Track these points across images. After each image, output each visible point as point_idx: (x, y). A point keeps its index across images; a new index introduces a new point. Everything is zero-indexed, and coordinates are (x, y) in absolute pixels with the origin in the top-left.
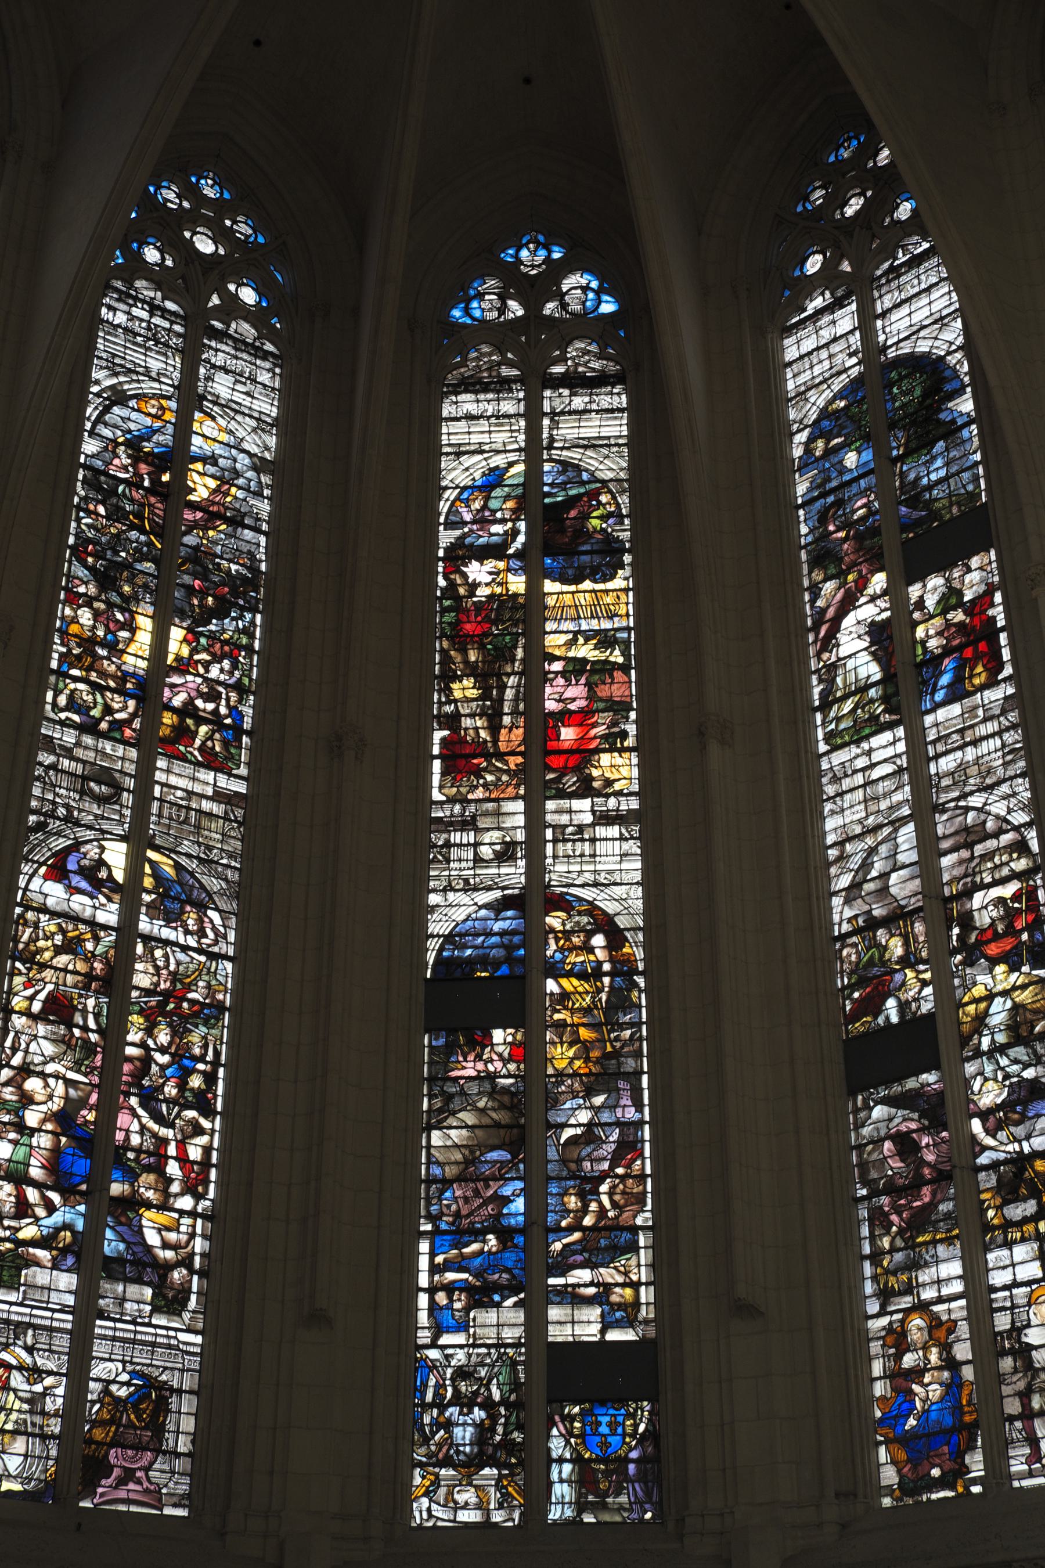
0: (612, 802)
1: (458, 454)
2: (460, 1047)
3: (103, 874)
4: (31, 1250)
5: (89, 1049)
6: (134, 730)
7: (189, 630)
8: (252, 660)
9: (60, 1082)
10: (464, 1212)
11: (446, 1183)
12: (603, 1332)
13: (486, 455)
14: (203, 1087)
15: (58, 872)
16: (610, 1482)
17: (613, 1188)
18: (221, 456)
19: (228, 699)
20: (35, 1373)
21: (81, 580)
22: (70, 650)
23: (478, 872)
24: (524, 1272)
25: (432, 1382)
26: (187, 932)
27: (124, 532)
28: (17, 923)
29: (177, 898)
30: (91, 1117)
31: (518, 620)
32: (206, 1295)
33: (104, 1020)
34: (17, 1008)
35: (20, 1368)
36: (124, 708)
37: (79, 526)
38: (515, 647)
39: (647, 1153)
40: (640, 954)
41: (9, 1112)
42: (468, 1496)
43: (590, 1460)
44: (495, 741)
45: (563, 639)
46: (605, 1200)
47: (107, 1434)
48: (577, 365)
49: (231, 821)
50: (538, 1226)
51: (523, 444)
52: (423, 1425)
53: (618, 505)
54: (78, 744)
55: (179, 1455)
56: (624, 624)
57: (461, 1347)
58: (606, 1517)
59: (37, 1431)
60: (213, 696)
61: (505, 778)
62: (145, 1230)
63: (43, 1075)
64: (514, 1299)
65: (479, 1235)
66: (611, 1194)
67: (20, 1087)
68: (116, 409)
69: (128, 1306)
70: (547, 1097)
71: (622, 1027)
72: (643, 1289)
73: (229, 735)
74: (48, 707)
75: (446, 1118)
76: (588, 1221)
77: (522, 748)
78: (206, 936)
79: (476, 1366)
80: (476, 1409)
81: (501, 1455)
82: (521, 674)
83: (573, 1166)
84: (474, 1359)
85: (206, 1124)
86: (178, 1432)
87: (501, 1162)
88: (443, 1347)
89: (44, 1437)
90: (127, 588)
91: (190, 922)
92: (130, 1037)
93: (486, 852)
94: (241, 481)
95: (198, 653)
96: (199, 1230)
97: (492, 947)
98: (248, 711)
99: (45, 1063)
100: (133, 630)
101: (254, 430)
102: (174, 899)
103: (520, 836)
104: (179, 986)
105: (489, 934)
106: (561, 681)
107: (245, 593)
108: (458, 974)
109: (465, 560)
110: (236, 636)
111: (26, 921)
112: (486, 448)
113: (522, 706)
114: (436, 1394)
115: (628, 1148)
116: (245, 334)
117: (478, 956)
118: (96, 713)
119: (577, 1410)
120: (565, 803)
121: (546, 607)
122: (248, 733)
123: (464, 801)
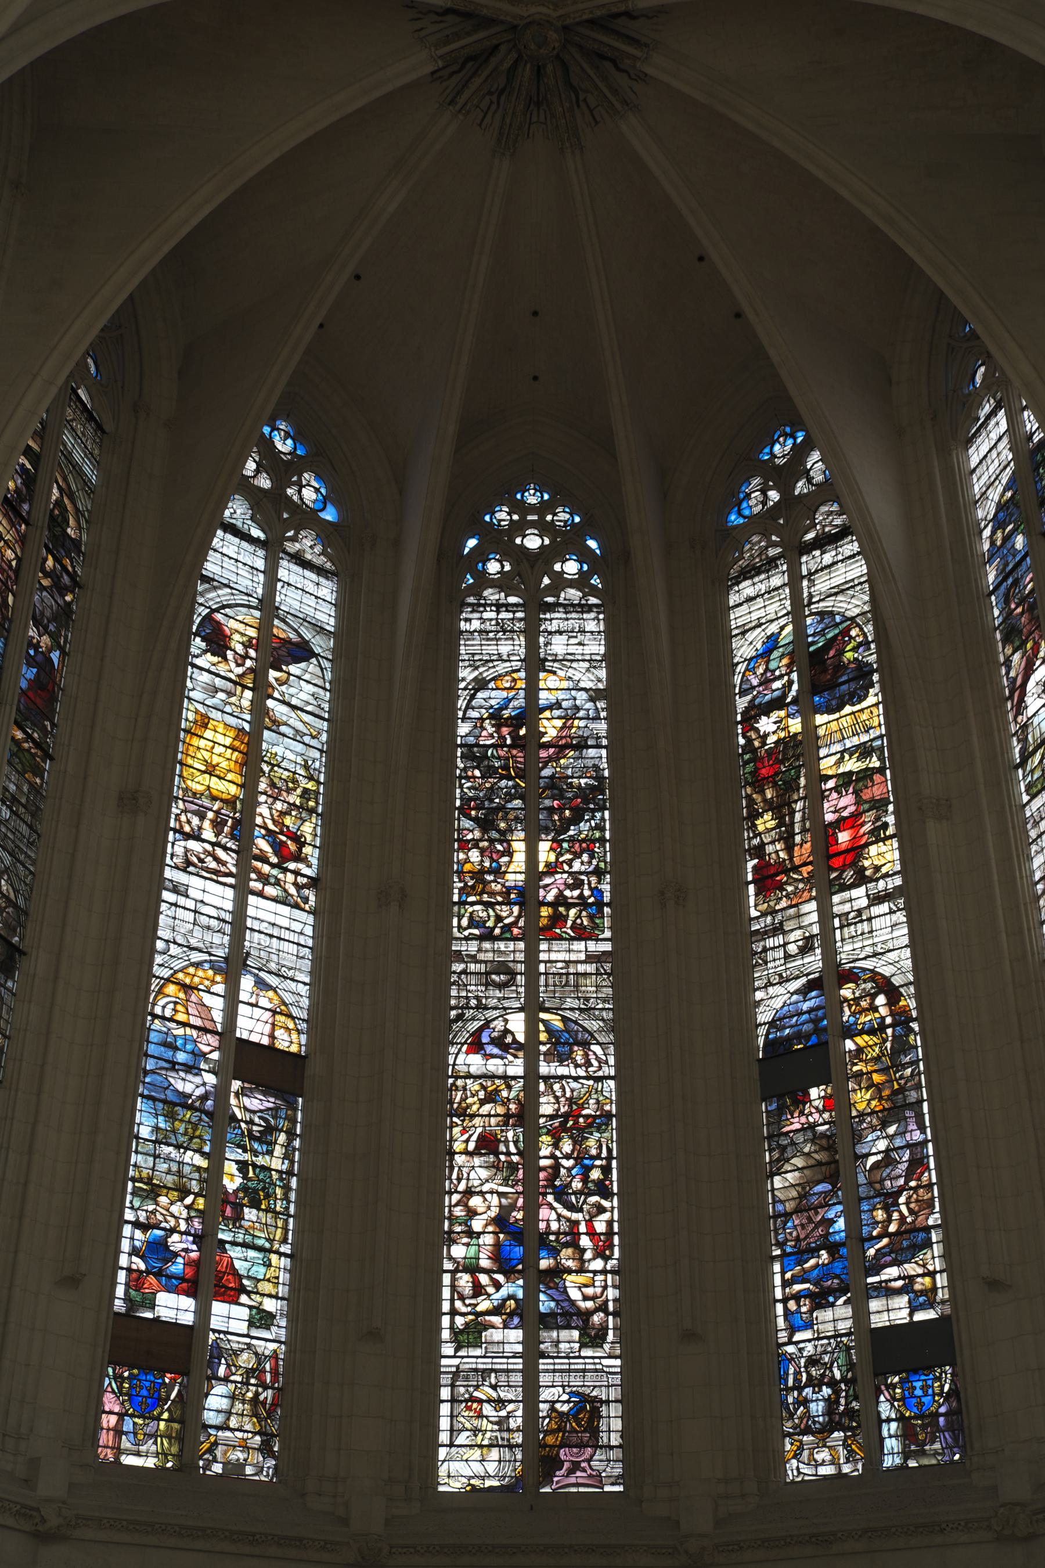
0: (881, 884)
1: (743, 633)
2: (788, 1107)
3: (509, 1039)
4: (487, 1318)
5: (513, 1167)
6: (520, 928)
7: (553, 840)
8: (605, 848)
9: (495, 1195)
10: (802, 1236)
11: (787, 1215)
12: (911, 1315)
13: (763, 627)
14: (601, 1177)
15: (476, 1046)
16: (926, 1434)
17: (909, 1198)
18: (563, 700)
19: (589, 883)
20: (500, 1403)
21: (468, 830)
22: (466, 884)
23: (788, 966)
24: (847, 1278)
25: (791, 1371)
26: (577, 1066)
27: (496, 783)
28: (451, 1090)
29: (564, 1044)
30: (520, 1215)
31: (799, 755)
33: (521, 1145)
34: (457, 1150)
35: (489, 1401)
36: (510, 914)
37: (462, 791)
38: (799, 777)
39: (932, 1165)
40: (912, 1004)
41: (460, 1224)
42: (823, 1455)
43: (910, 1418)
44: (791, 858)
45: (833, 760)
46: (904, 1209)
48: (824, 527)
49: (601, 974)
50: (858, 1238)
51: (789, 608)
52: (788, 1404)
53: (865, 635)
54: (480, 950)
55: (611, 1448)
56: (878, 733)
57: (809, 1341)
58: (926, 1461)
59: (506, 1443)
60: (578, 884)
61: (801, 886)
63: (482, 1193)
64: (844, 1298)
65: (814, 1252)
66: (907, 1204)
67: (466, 1205)
68: (479, 695)
69: (562, 1346)
70: (853, 1135)
71: (904, 1067)
72: (938, 1276)
73: (593, 910)
74: (455, 930)
75: (783, 1165)
76: (893, 1228)
77: (811, 858)
78: (592, 1065)
79: (821, 1354)
80: (824, 1388)
81: (845, 1421)
82: (804, 798)
83: (877, 1186)
84: (819, 1349)
85: (606, 1204)
86: (609, 1431)
87: (825, 1192)
88: (797, 1343)
89: (511, 1447)
90: (503, 825)
91: (578, 1058)
92: (542, 1153)
93: (792, 949)
94: (581, 714)
95: (562, 855)
96: (609, 1283)
97: (803, 1024)
98: (606, 887)
99: (482, 1185)
100: (509, 853)
101: (588, 670)
102: (564, 1044)
103: (816, 930)
104: (575, 1107)
105: (800, 1014)
106: (835, 795)
107: (594, 798)
108: (781, 1050)
109: (756, 718)
110: (591, 833)
111: (457, 1087)
112: (763, 621)
113: (808, 825)
114: (795, 1380)
115: (917, 1164)
116: (572, 598)
117: (794, 1033)
118: (490, 924)
119: (897, 1379)
120: (846, 895)
121: (818, 738)
122: (608, 905)
123: (773, 912)
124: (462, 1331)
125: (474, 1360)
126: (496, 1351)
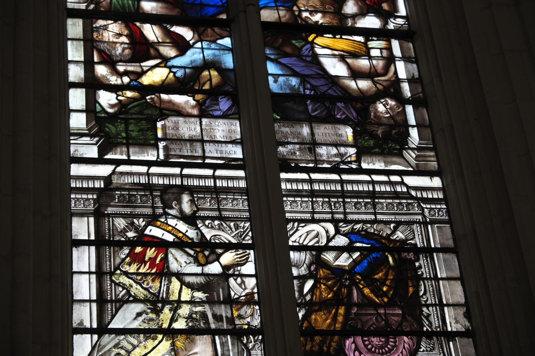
4: (164, 96)
20: (205, 250)
32: (430, 126)
35: (181, 244)
47: (335, 319)
55: (451, 336)
62: (323, 60)
86: (441, 305)
89: (238, 334)
96: (397, 51)
124: (111, 118)
125: (143, 169)
126: (185, 153)
